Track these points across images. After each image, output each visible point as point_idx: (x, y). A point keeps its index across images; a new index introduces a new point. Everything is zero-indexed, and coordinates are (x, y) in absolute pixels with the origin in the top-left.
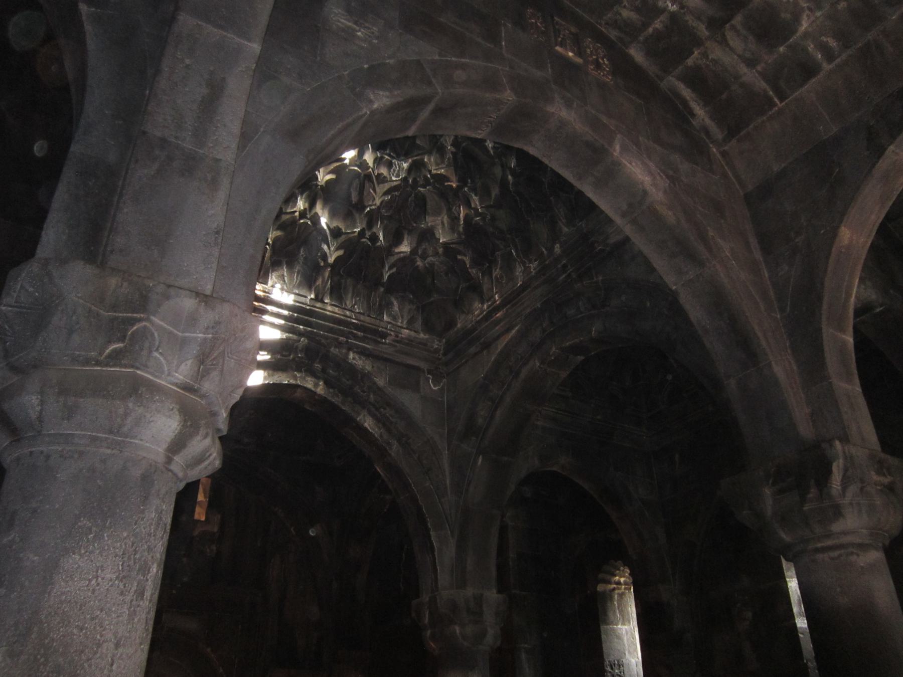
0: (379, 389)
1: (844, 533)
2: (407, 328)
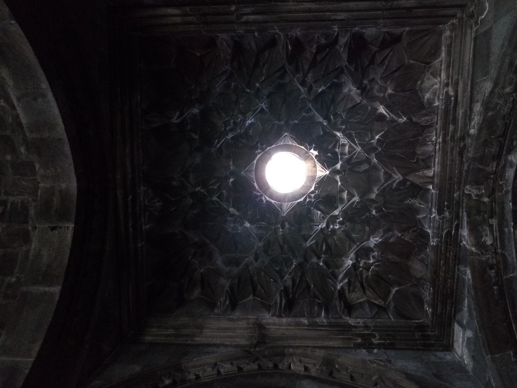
2: (440, 75)
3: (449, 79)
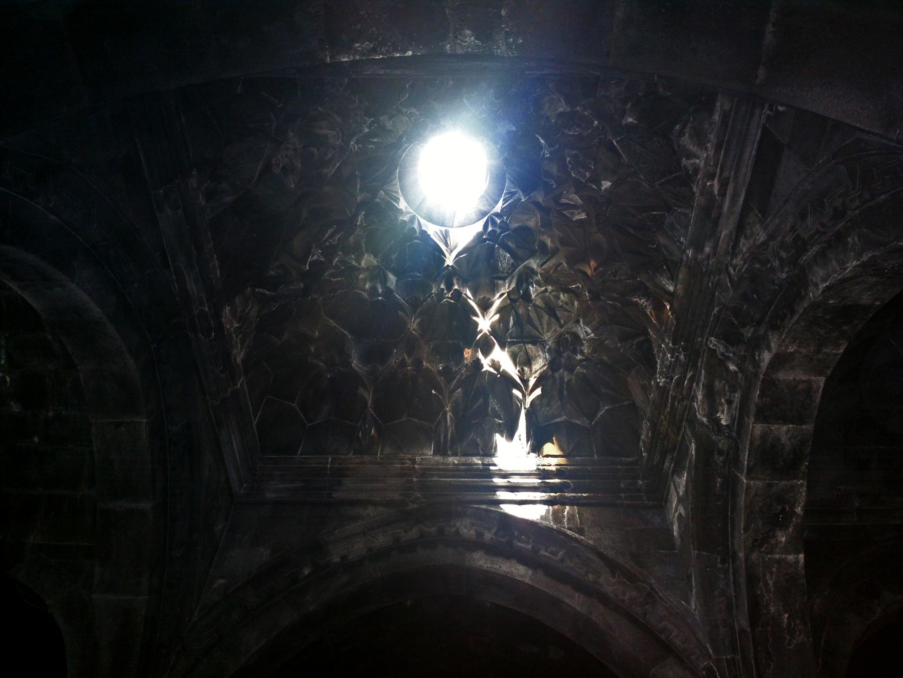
0: (771, 237)
3: (717, 168)
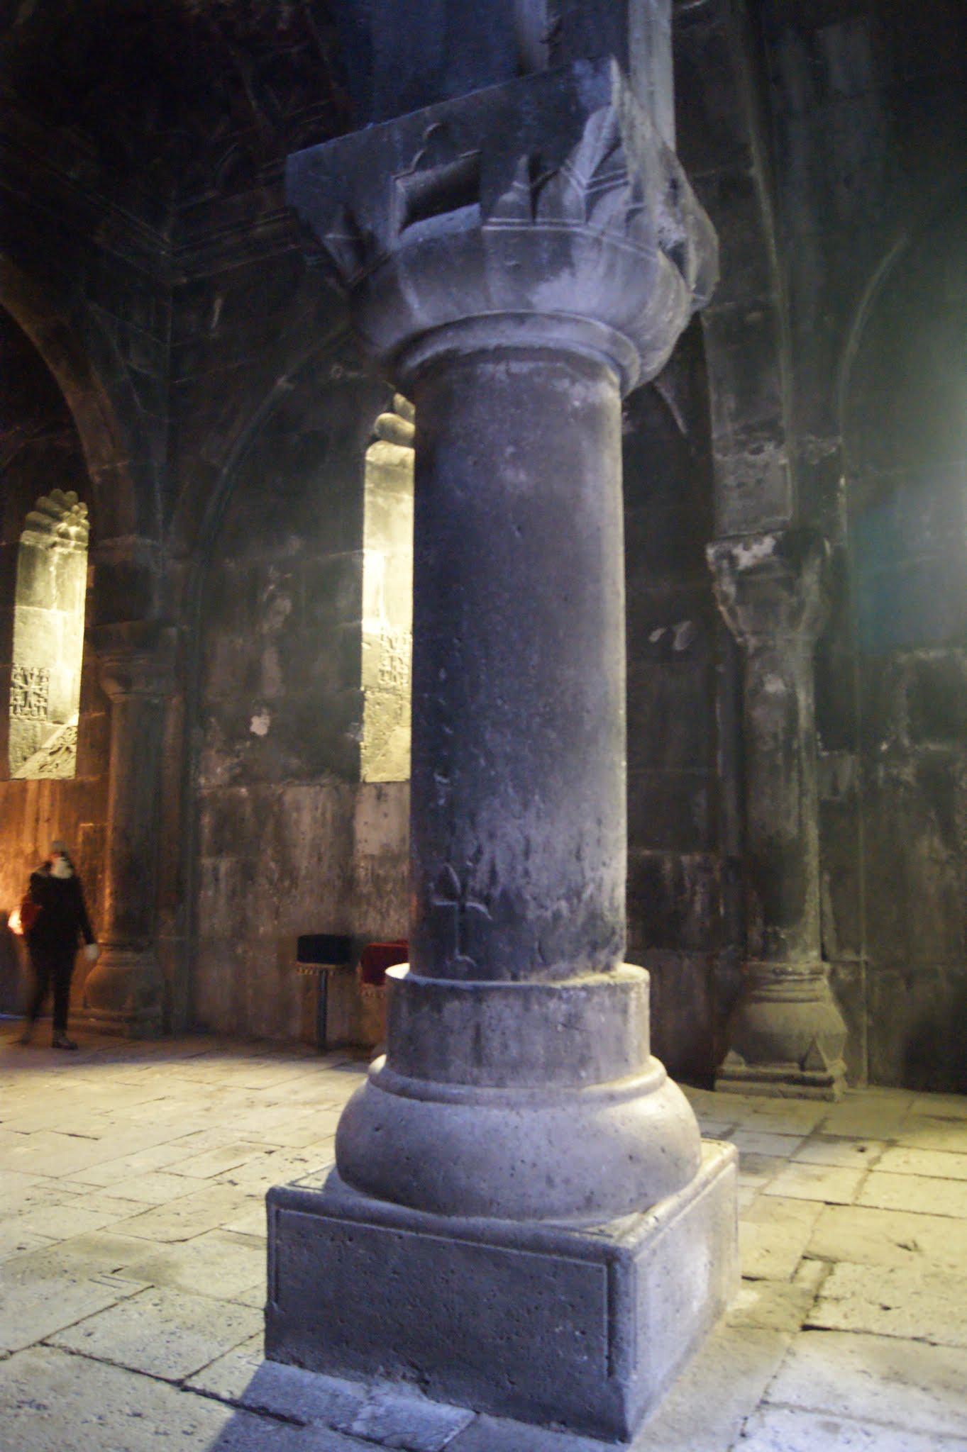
1: (557, 318)
